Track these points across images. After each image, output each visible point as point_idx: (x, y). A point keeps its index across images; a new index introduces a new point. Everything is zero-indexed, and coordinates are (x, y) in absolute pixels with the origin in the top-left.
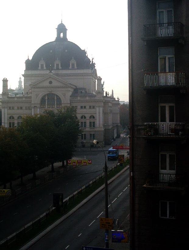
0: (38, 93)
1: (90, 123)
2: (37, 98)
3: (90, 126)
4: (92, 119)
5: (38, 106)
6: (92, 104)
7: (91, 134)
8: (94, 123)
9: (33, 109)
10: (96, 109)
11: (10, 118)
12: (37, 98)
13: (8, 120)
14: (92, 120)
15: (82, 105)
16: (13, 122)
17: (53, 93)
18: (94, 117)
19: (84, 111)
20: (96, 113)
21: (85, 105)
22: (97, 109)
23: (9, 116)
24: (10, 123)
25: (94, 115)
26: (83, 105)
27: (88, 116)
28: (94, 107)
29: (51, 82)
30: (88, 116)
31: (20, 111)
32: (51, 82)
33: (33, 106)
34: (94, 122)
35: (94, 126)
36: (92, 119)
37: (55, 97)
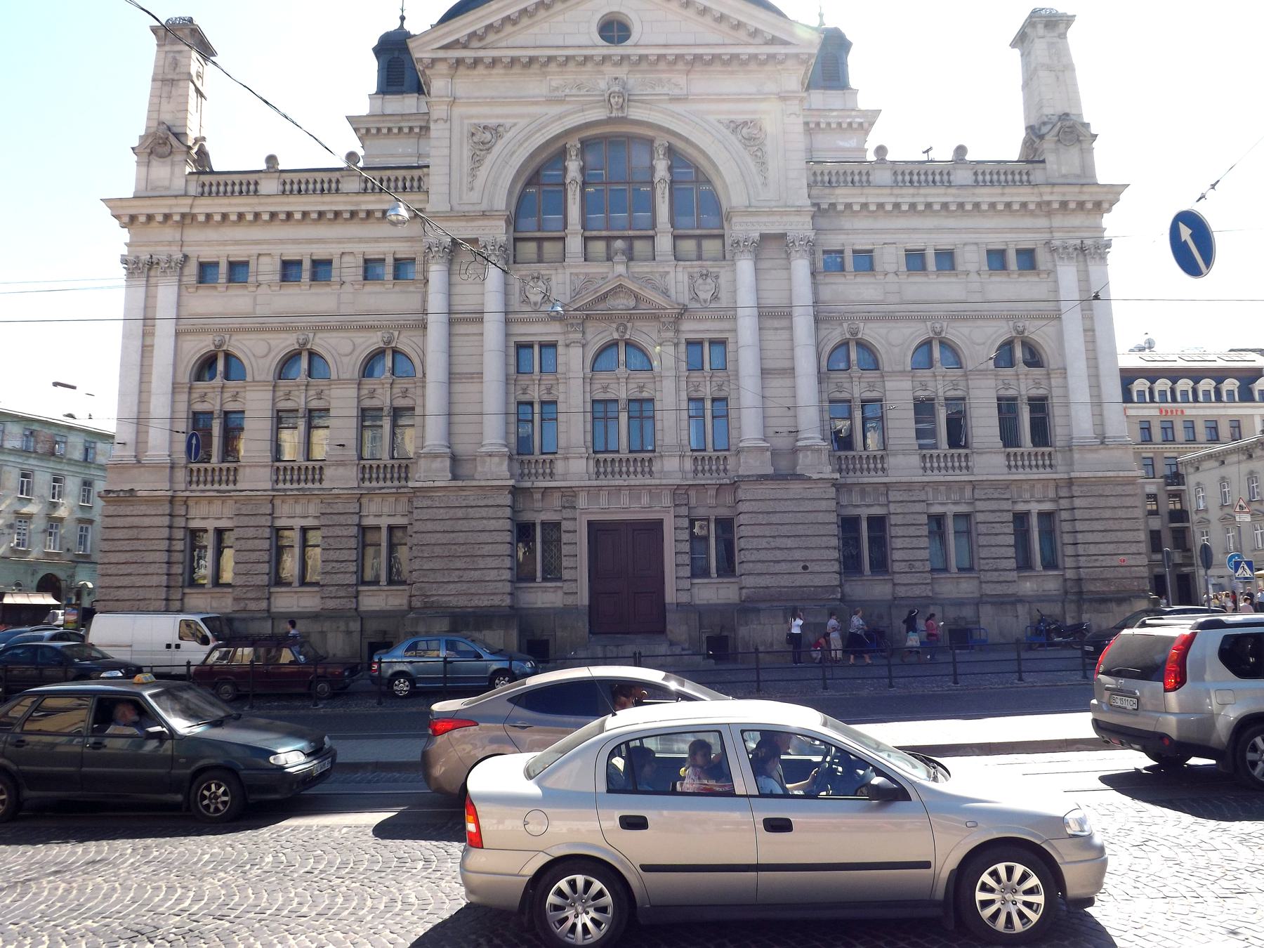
0: (492, 122)
1: (1007, 408)
2: (477, 161)
3: (1009, 435)
5: (497, 232)
7: (1027, 514)
8: (1039, 406)
9: (436, 273)
11: (206, 366)
12: (477, 161)
14: (1024, 383)
15: (916, 242)
16: (230, 406)
17: (636, 113)
18: (1034, 359)
19: (935, 288)
23: (199, 346)
24: (199, 421)
30: (979, 342)
31: (304, 299)
33: (441, 233)
34: (1044, 398)
35: (1041, 432)
36: (1022, 368)
37: (661, 167)
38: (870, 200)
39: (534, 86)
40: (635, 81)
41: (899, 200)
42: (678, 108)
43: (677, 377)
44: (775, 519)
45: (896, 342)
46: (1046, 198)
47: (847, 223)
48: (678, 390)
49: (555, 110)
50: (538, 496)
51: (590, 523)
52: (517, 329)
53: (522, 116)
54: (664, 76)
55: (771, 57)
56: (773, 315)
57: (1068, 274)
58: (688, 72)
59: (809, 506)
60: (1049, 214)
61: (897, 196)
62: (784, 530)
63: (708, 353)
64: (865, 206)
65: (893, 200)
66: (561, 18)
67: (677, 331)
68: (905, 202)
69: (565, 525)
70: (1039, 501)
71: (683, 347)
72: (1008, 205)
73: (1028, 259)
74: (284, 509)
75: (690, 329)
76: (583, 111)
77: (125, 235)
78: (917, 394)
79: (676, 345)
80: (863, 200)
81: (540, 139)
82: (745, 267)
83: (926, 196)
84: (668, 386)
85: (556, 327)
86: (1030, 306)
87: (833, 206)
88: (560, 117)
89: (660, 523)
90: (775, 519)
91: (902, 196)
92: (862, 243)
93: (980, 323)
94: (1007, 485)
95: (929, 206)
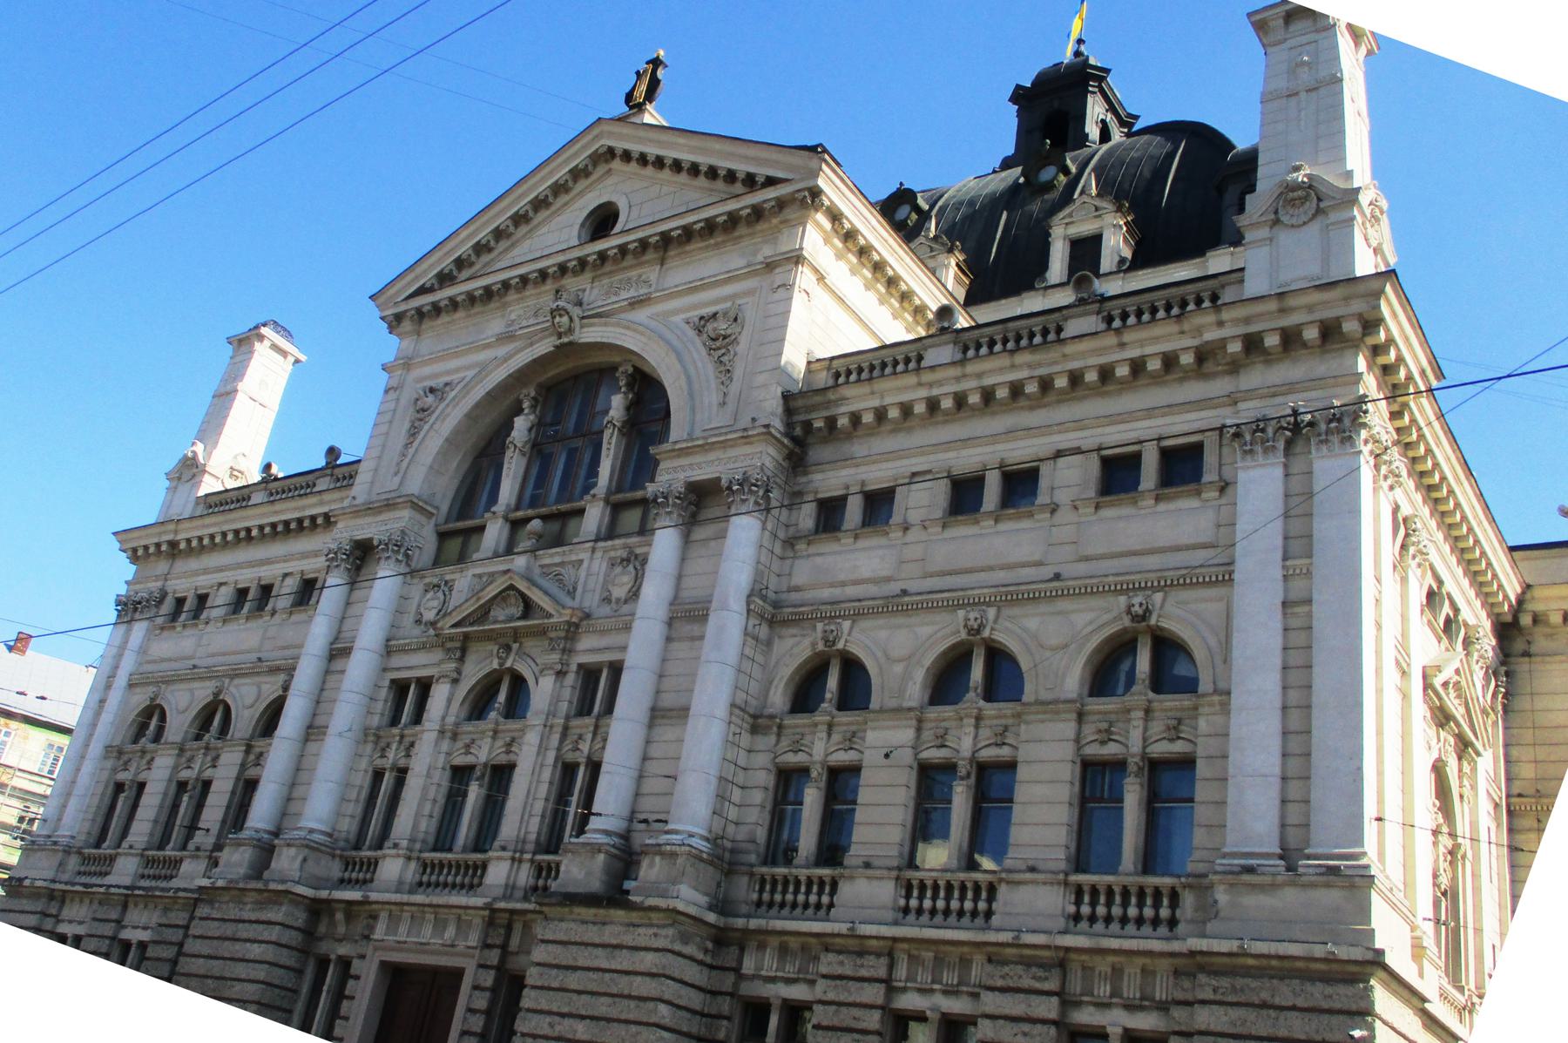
0: (438, 383)
4: (1141, 693)
6: (1145, 420)
10: (1224, 487)
12: (413, 432)
13: (108, 748)
14: (1137, 729)
17: (590, 334)
20: (1224, 577)
21: (1019, 452)
22: (1259, 484)
23: (140, 699)
25: (1179, 615)
26: (985, 446)
27: (1055, 647)
28: (1182, 465)
29: (603, 221)
30: (1055, 647)
32: (603, 221)
34: (1186, 764)
38: (888, 400)
39: (494, 324)
40: (594, 291)
41: (935, 392)
42: (641, 315)
43: (548, 726)
44: (573, 980)
45: (899, 654)
46: (1211, 335)
47: (858, 448)
48: (542, 749)
49: (501, 351)
50: (339, 916)
51: (384, 965)
52: (397, 661)
53: (468, 368)
54: (634, 273)
55: (758, 213)
56: (687, 615)
57: (1259, 484)
58: (662, 262)
59: (623, 961)
60: (1234, 367)
61: (930, 385)
62: (581, 1004)
63: (595, 689)
64: (881, 414)
65: (923, 393)
66: (544, 230)
67: (568, 652)
68: (945, 393)
69: (356, 963)
70: (1130, 1007)
71: (570, 679)
72: (1137, 367)
73: (1182, 465)
74: (135, 915)
75: (589, 649)
76: (531, 344)
77: (129, 570)
78: (924, 755)
79: (560, 674)
80: (876, 403)
81: (479, 393)
82: (664, 543)
83: (979, 376)
84: (532, 738)
85: (437, 655)
86: (1152, 562)
87: (831, 422)
88: (506, 360)
89: (458, 974)
90: (573, 980)
91: (940, 383)
92: (877, 476)
93: (1063, 605)
94: (1061, 961)
95: (988, 395)
